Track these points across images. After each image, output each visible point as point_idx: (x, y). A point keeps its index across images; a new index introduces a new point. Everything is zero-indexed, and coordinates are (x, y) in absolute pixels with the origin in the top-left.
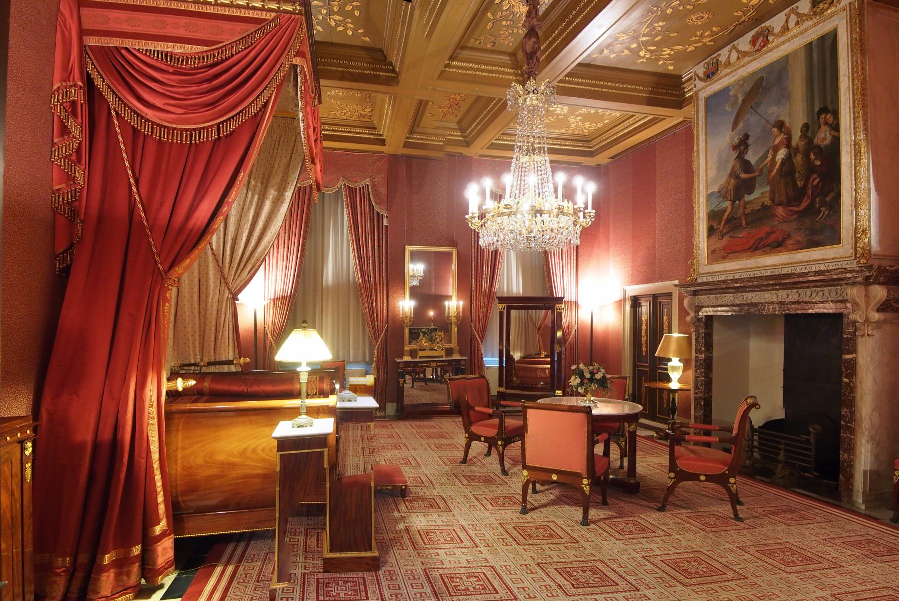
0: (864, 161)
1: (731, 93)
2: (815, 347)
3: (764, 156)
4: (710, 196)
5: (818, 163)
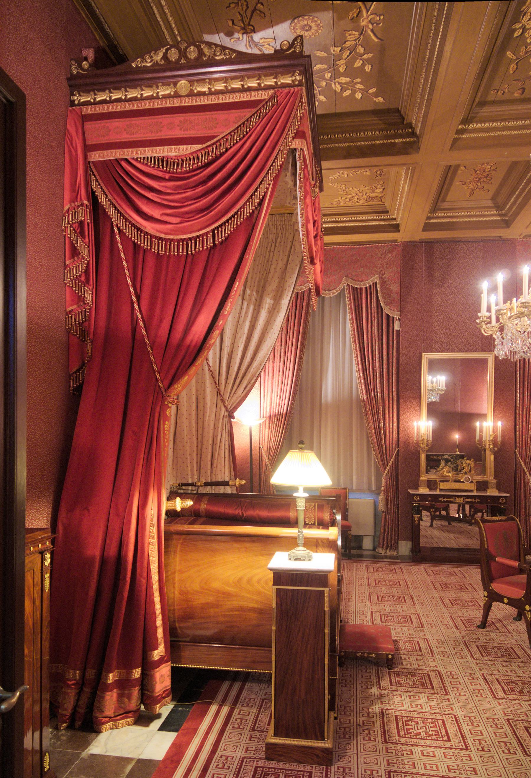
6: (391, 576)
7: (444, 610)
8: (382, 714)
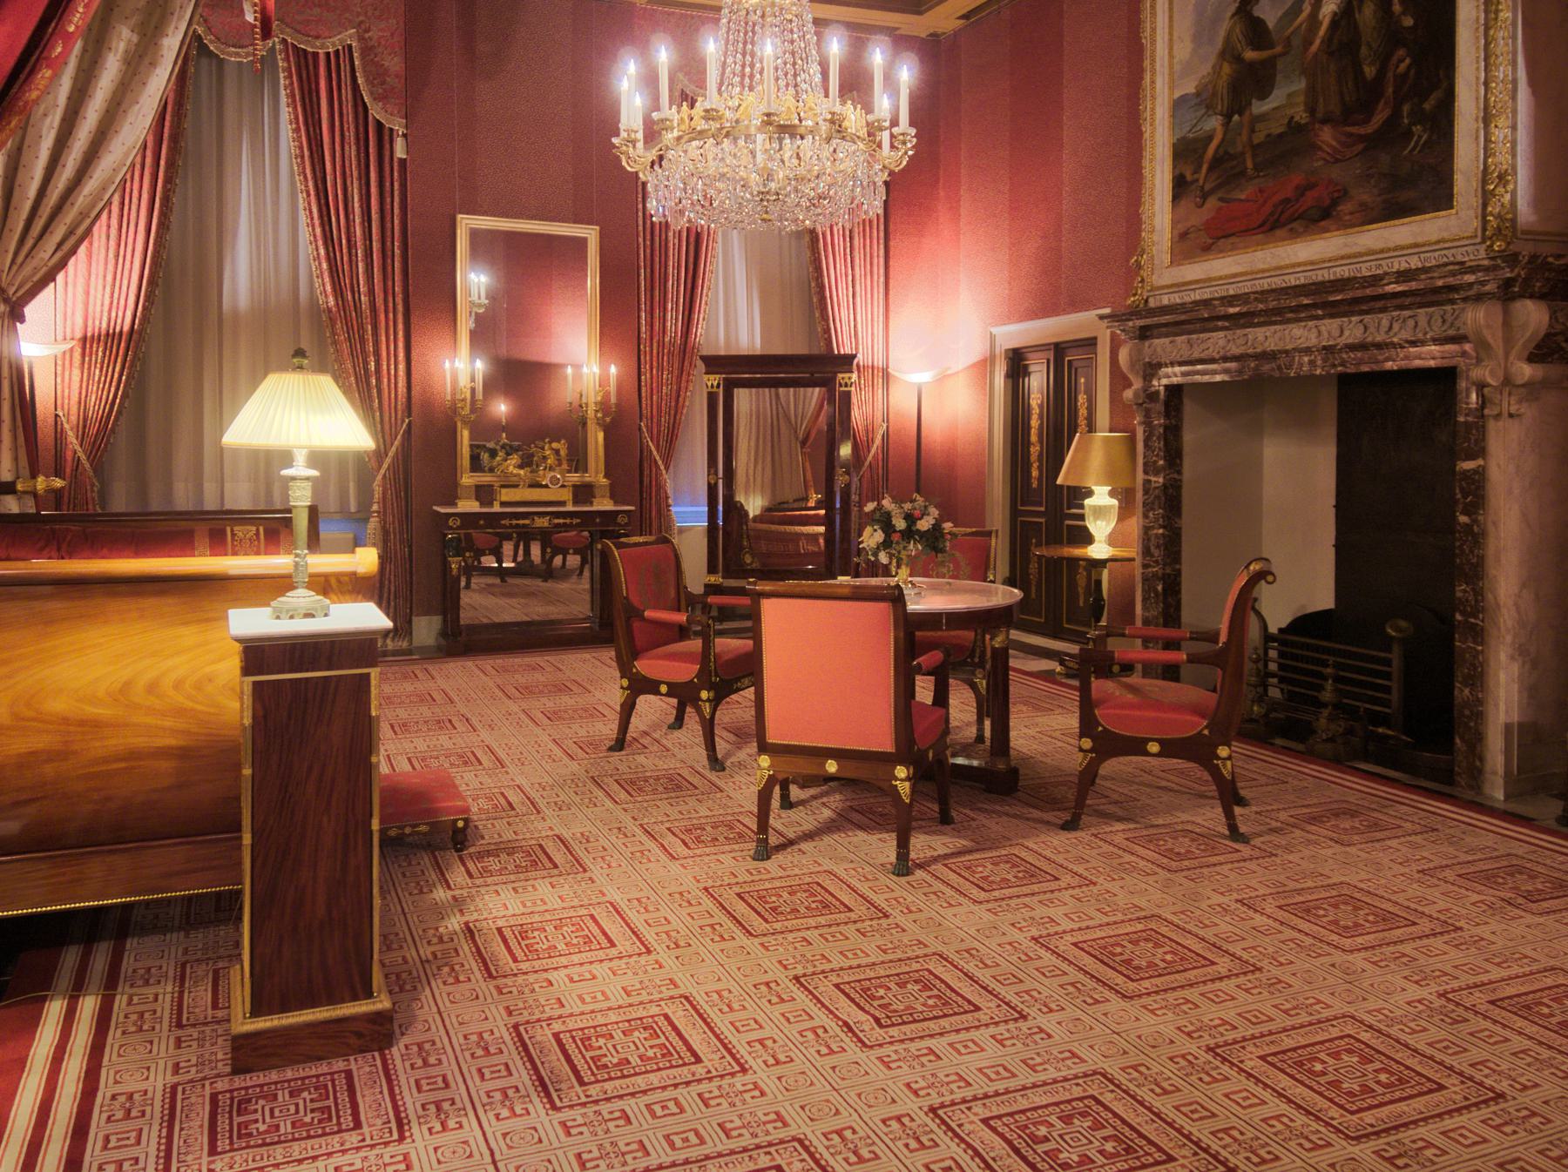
0: (1506, 15)
2: (1399, 439)
3: (1295, 10)
4: (1178, 105)
6: (408, 687)
7: (538, 731)
8: (469, 931)
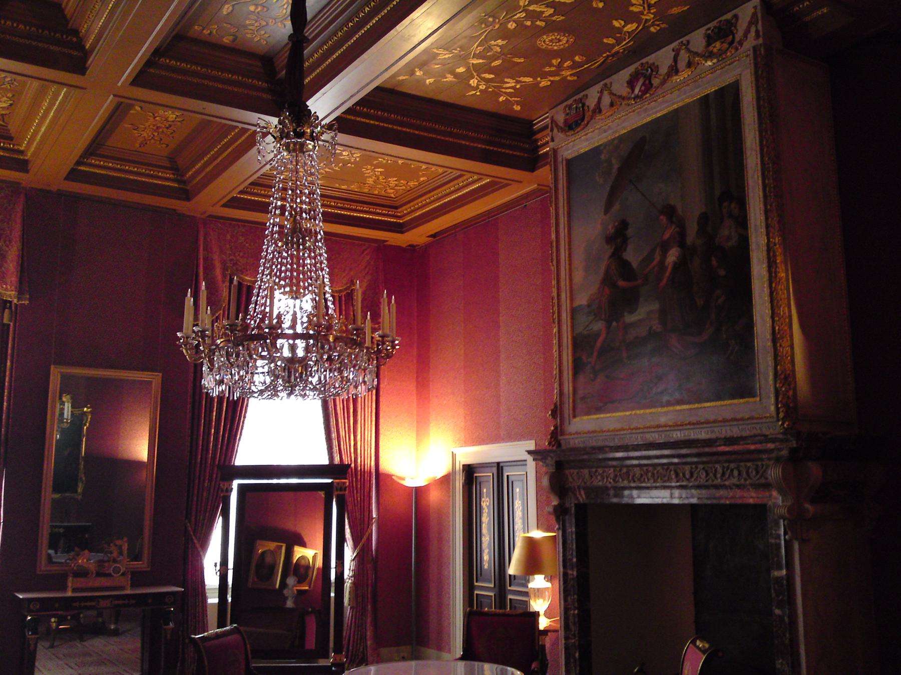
1: (603, 157)
3: (649, 258)
5: (722, 273)
